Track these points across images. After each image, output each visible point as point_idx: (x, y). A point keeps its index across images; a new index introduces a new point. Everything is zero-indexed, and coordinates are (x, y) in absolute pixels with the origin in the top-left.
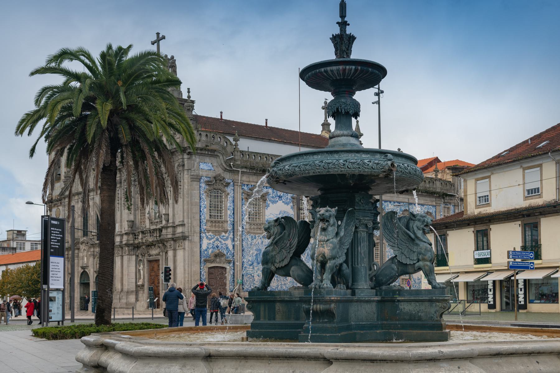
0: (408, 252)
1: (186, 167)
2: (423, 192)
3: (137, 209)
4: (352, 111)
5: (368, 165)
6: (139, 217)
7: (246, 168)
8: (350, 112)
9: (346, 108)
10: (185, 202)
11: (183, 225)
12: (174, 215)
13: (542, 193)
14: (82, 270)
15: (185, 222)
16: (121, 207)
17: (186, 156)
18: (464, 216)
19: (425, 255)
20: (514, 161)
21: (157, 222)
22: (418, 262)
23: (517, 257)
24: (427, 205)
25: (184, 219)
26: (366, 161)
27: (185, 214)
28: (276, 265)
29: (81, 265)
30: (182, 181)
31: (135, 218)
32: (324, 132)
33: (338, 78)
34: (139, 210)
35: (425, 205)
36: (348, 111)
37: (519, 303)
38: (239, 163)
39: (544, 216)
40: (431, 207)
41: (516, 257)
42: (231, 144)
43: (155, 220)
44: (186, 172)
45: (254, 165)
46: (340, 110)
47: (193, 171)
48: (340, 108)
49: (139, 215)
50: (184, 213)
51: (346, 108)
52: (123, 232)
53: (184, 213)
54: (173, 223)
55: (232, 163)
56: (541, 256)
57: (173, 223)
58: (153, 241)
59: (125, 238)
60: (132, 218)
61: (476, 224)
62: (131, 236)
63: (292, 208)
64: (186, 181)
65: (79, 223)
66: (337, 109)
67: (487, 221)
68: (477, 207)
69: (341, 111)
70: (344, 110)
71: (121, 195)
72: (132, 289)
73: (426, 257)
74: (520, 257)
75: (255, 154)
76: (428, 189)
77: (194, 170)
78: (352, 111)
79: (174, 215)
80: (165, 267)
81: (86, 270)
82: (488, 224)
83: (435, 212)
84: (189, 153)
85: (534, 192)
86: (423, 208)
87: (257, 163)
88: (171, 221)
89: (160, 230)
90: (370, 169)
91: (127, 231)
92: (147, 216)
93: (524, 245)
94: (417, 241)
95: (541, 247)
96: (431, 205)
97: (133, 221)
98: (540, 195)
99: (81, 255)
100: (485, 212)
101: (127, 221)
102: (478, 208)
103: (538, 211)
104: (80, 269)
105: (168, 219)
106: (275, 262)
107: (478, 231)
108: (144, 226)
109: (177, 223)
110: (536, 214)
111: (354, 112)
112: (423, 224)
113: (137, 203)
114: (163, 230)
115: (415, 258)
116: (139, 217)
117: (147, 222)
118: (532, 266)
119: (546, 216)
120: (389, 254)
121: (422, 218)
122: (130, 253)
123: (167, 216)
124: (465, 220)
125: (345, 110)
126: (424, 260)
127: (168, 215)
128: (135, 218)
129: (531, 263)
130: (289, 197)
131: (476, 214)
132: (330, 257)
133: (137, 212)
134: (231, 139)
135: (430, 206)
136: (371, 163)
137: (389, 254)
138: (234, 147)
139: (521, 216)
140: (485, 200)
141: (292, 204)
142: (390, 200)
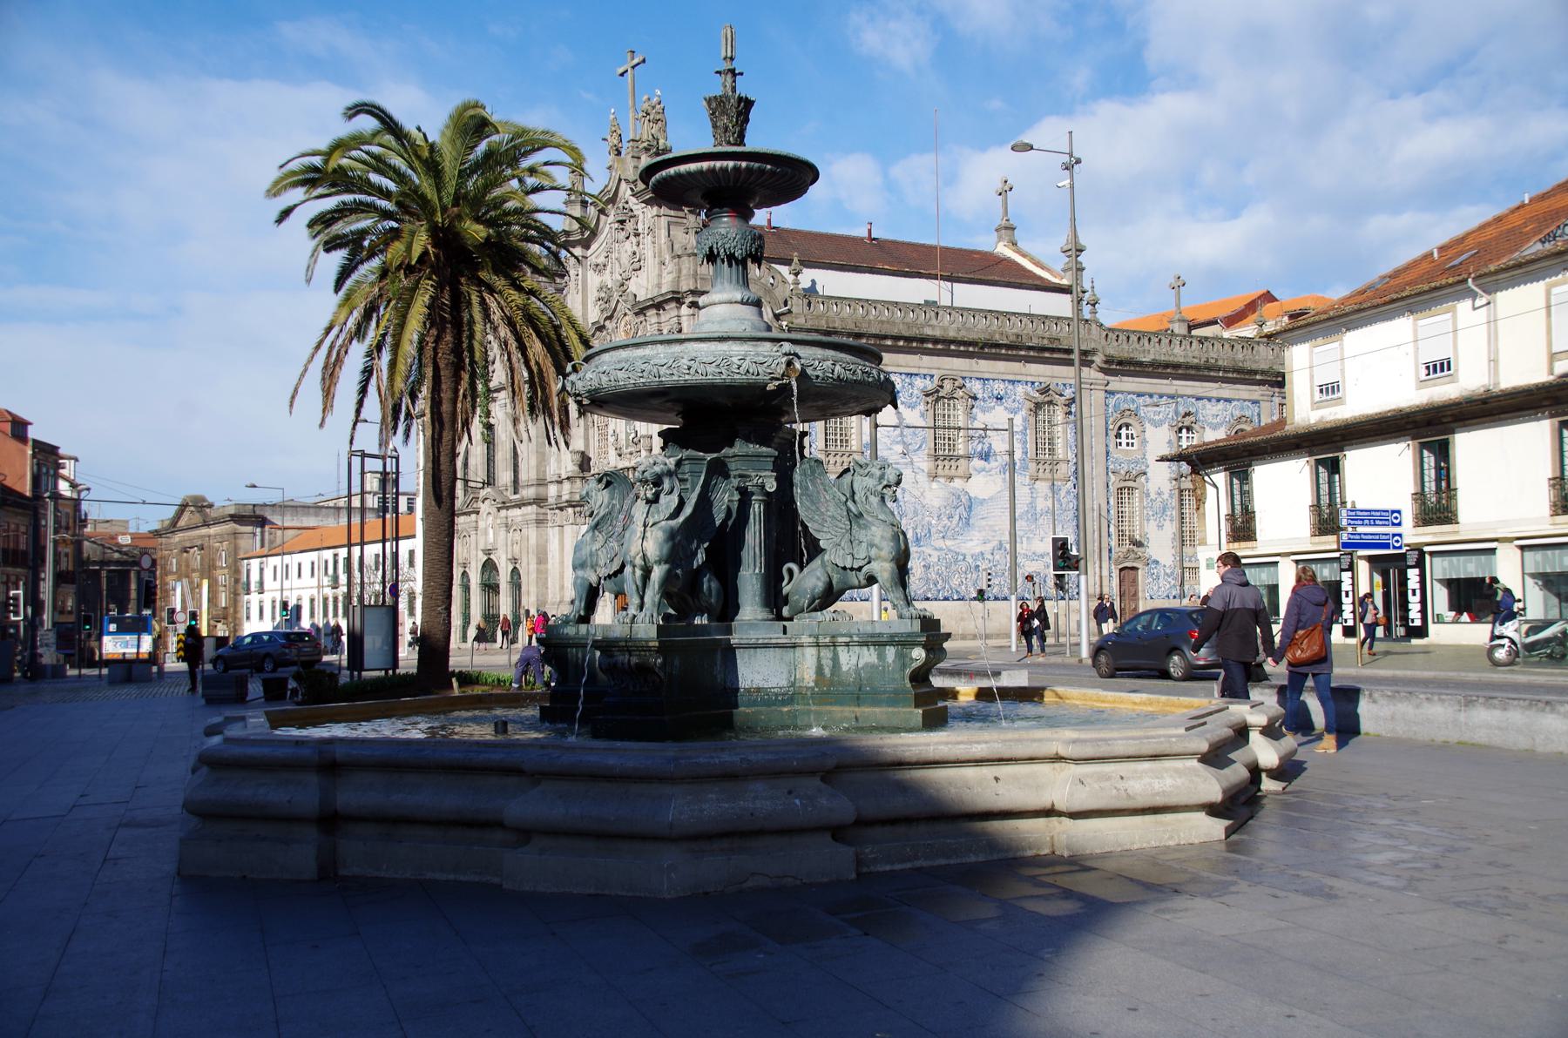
2: (1229, 372)
3: (591, 425)
7: (817, 331)
9: (727, 246)
13: (1456, 371)
14: (485, 558)
17: (685, 310)
18: (1287, 428)
20: (1393, 301)
21: (631, 454)
22: (869, 562)
23: (1360, 522)
24: (1238, 400)
26: (735, 360)
28: (598, 570)
29: (481, 546)
31: (587, 445)
32: (1001, 244)
34: (596, 429)
35: (1234, 400)
37: (1411, 624)
38: (800, 321)
39: (1461, 423)
40: (1249, 404)
41: (1356, 522)
42: (785, 281)
45: (836, 325)
48: (715, 246)
49: (596, 438)
51: (727, 246)
52: (564, 476)
55: (784, 323)
56: (1456, 515)
59: (567, 486)
61: (1314, 445)
62: (578, 480)
63: (922, 415)
65: (479, 459)
66: (711, 248)
67: (1338, 438)
68: (1316, 405)
69: (718, 252)
74: (1366, 522)
75: (839, 301)
76: (1241, 364)
78: (740, 251)
81: (492, 557)
82: (1339, 444)
83: (1259, 415)
84: (694, 305)
85: (1440, 367)
86: (1229, 407)
87: (843, 320)
91: (570, 474)
92: (611, 439)
93: (1419, 490)
95: (1456, 495)
96: (1249, 401)
97: (583, 453)
98: (1451, 375)
99: (482, 524)
100: (1332, 418)
102: (1317, 409)
103: (1449, 413)
104: (480, 554)
106: (597, 565)
107: (1318, 462)
108: (605, 462)
110: (1445, 420)
111: (744, 253)
117: (612, 453)
118: (1397, 541)
119: (1467, 422)
120: (1151, 513)
122: (578, 520)
123: (648, 440)
124: (1286, 438)
128: (587, 445)
129: (1394, 535)
130: (916, 392)
131: (1312, 421)
133: (591, 431)
134: (784, 270)
135: (1246, 403)
137: (1151, 513)
138: (792, 287)
139: (1409, 427)
140: (1330, 389)
141: (922, 407)
142: (1151, 391)
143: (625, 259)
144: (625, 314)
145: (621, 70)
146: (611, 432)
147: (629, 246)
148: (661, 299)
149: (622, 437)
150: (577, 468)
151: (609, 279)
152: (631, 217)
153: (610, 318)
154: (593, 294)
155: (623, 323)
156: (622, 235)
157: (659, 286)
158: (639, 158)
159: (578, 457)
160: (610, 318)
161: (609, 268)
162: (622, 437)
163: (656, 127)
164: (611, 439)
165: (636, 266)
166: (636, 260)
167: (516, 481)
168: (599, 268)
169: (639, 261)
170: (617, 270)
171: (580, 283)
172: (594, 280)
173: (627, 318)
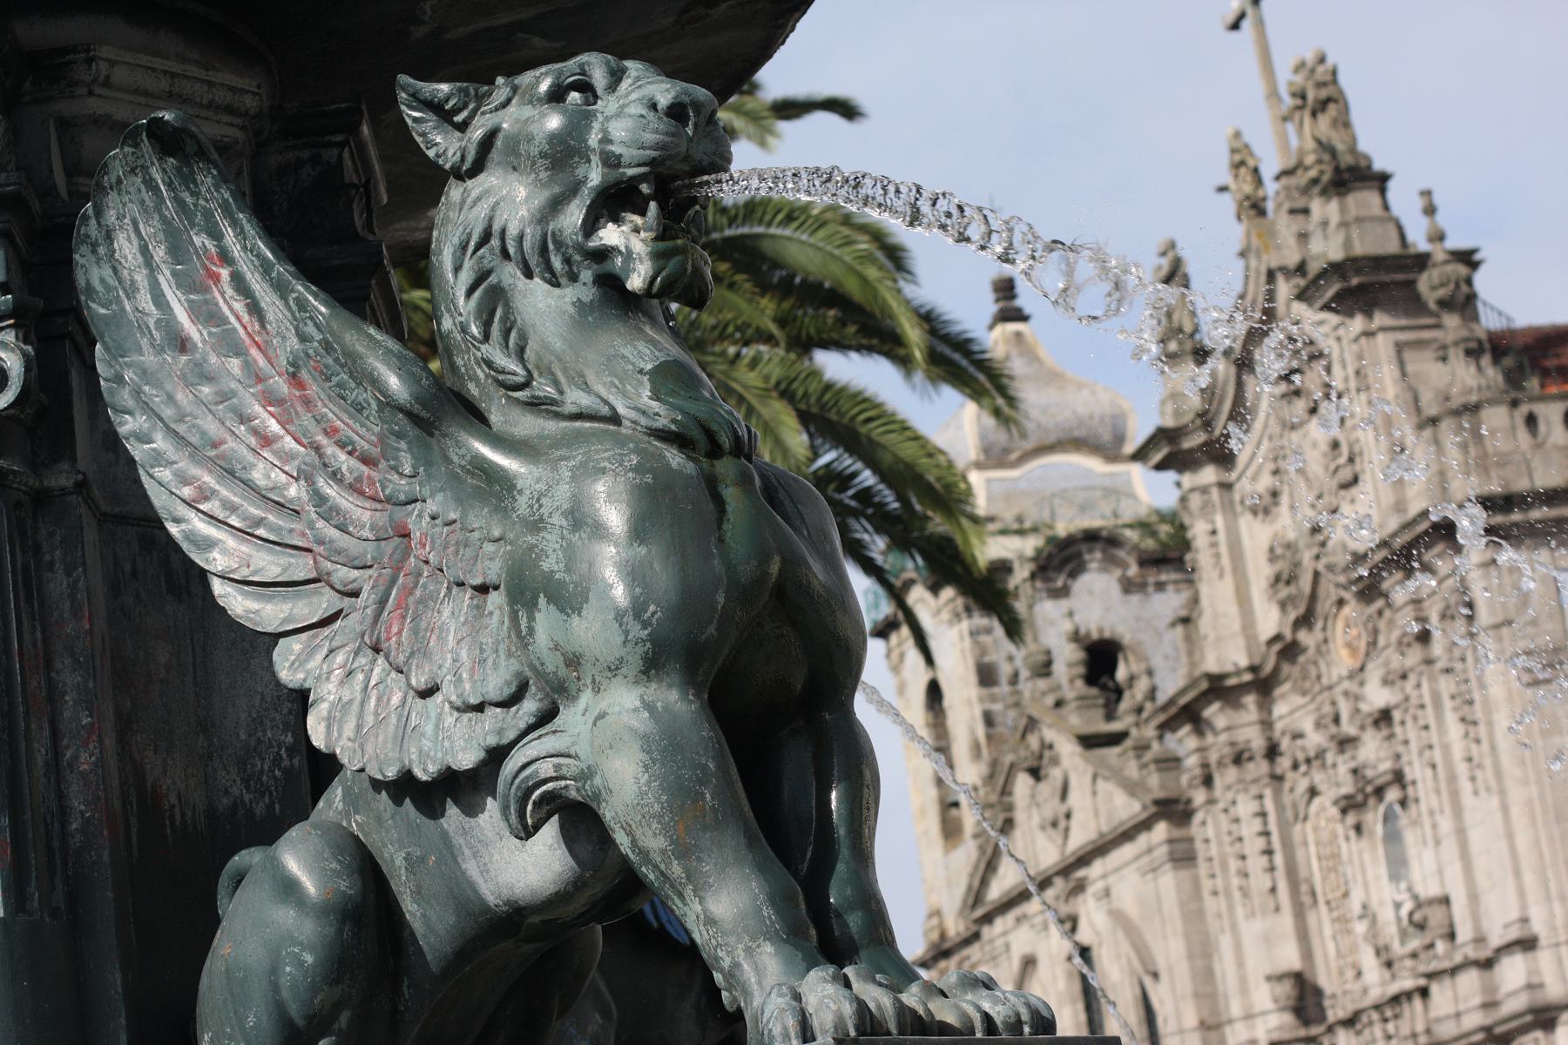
1: (1484, 616)
6: (1331, 947)
10: (1516, 811)
11: (1527, 944)
12: (1474, 898)
15: (1538, 927)
16: (1231, 908)
21: (1414, 955)
25: (1524, 905)
27: (1529, 878)
30: (1477, 696)
31: (1307, 953)
34: (1323, 908)
43: (1403, 942)
44: (1487, 642)
47: (1530, 630)
50: (1517, 874)
53: (1517, 874)
54: (1480, 940)
57: (1480, 940)
60: (1290, 958)
64: (1496, 691)
71: (1220, 844)
77: (1534, 622)
79: (1474, 898)
88: (1464, 933)
101: (1269, 978)
105: (1451, 925)
109: (1496, 941)
113: (1303, 873)
114: (1435, 989)
116: (1327, 947)
127: (1445, 901)
128: (1307, 953)
133: (1311, 919)
143: (1315, 462)
144: (1341, 603)
146: (1356, 908)
147: (1317, 433)
148: (1407, 537)
149: (1387, 915)
150: (1288, 1018)
151: (1288, 523)
152: (1312, 358)
153: (1305, 621)
154: (1260, 573)
155: (1340, 625)
156: (1301, 405)
157: (1400, 507)
158: (1306, 211)
159: (1286, 988)
160: (1305, 621)
161: (1285, 499)
162: (1387, 915)
163: (1324, 121)
164: (1360, 928)
165: (1346, 474)
166: (1342, 460)
168: (1265, 508)
169: (1351, 460)
170: (1306, 496)
171: (1223, 549)
172: (1256, 536)
173: (1347, 611)
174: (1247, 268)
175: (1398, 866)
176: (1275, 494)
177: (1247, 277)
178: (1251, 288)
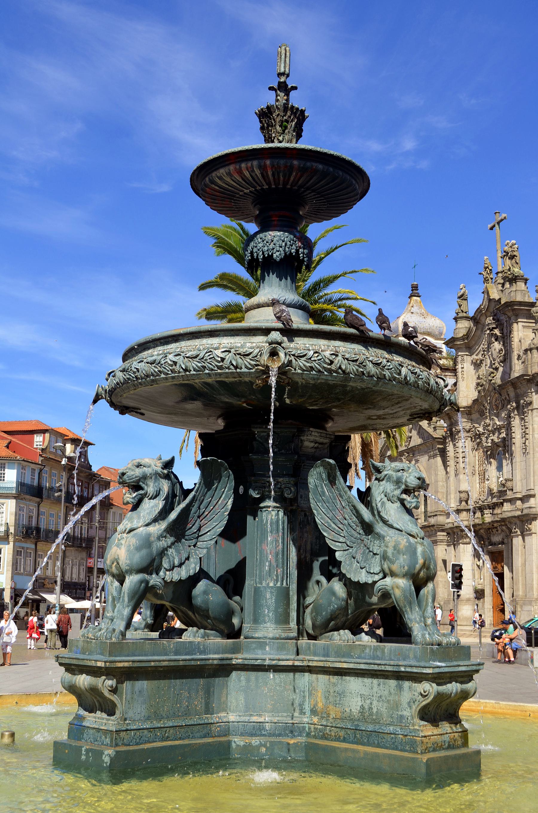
0: (364, 553)
4: (278, 253)
5: (223, 359)
8: (275, 256)
19: (393, 563)
30: (530, 427)
33: (266, 187)
36: (270, 254)
46: (255, 254)
58: (492, 522)
70: (261, 253)
72: (468, 596)
73: (395, 568)
80: (453, 564)
89: (502, 504)
90: (228, 368)
94: (380, 528)
97: (467, 492)
112: (399, 488)
114: (505, 504)
115: (377, 569)
121: (394, 474)
125: (263, 253)
126: (393, 574)
132: (127, 568)
136: (230, 354)
145: (490, 226)
167: (426, 512)
171: (465, 373)
174: (484, 297)
175: (500, 468)
176: (481, 361)
177: (484, 300)
178: (484, 303)
